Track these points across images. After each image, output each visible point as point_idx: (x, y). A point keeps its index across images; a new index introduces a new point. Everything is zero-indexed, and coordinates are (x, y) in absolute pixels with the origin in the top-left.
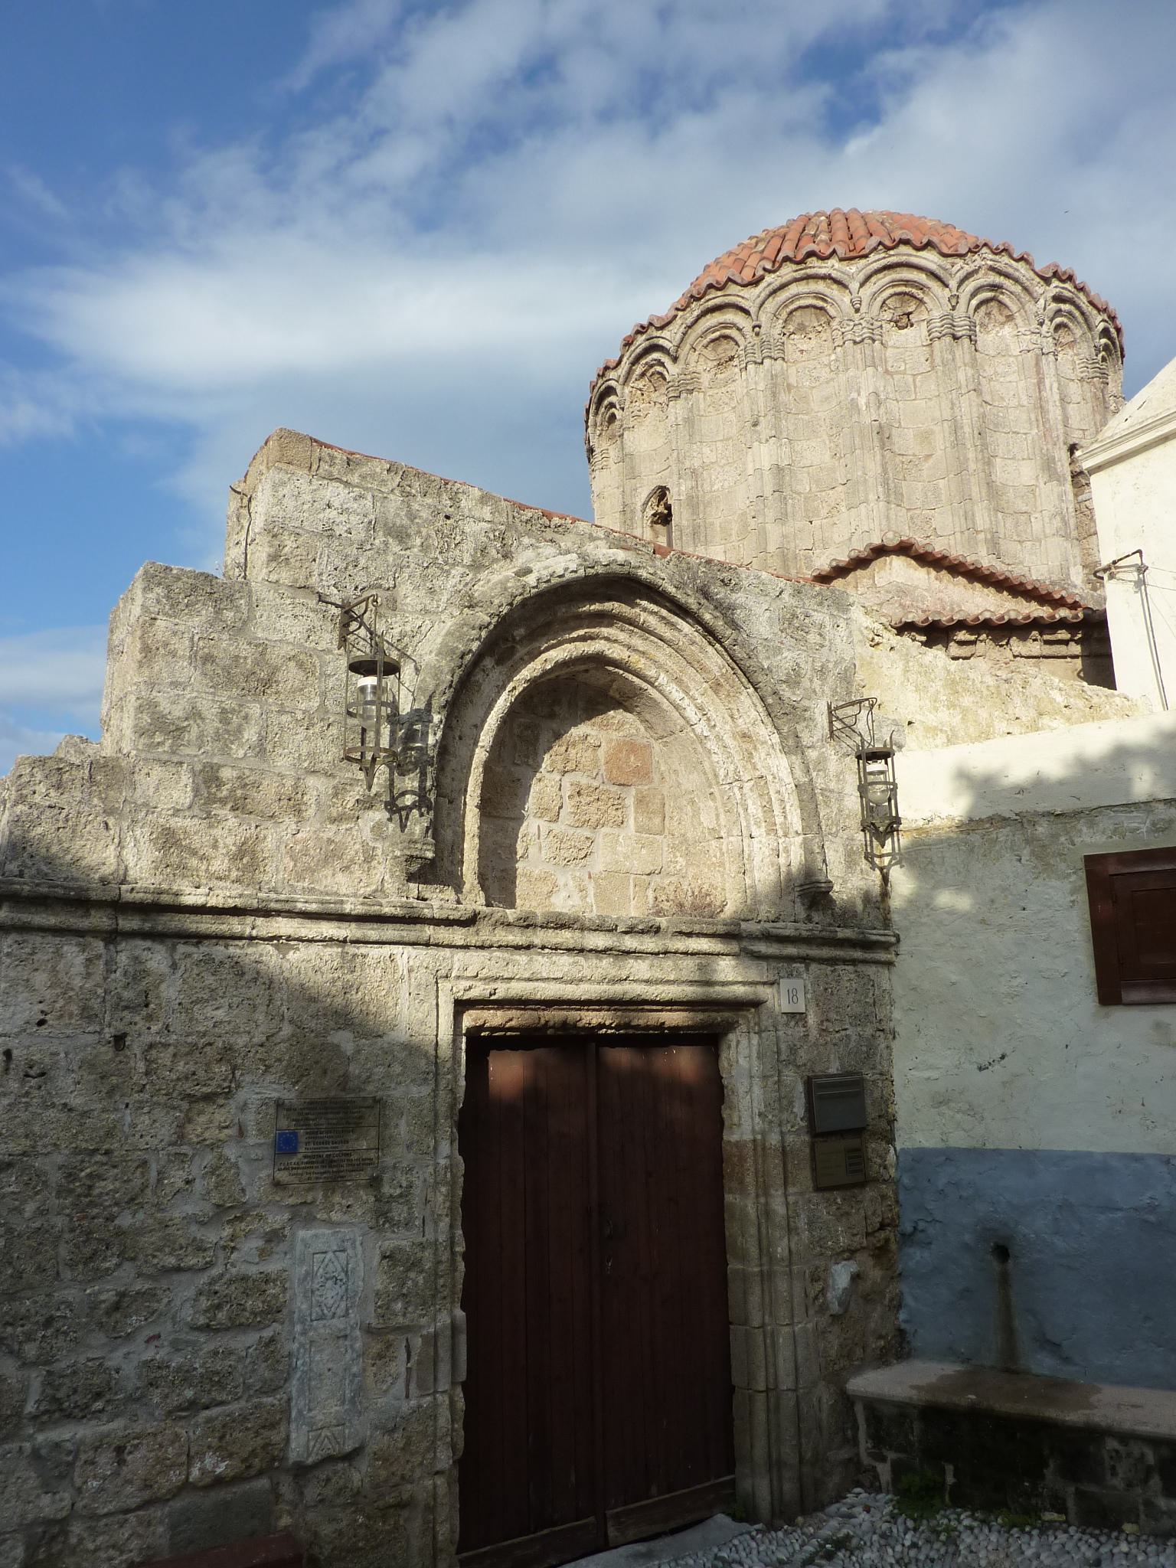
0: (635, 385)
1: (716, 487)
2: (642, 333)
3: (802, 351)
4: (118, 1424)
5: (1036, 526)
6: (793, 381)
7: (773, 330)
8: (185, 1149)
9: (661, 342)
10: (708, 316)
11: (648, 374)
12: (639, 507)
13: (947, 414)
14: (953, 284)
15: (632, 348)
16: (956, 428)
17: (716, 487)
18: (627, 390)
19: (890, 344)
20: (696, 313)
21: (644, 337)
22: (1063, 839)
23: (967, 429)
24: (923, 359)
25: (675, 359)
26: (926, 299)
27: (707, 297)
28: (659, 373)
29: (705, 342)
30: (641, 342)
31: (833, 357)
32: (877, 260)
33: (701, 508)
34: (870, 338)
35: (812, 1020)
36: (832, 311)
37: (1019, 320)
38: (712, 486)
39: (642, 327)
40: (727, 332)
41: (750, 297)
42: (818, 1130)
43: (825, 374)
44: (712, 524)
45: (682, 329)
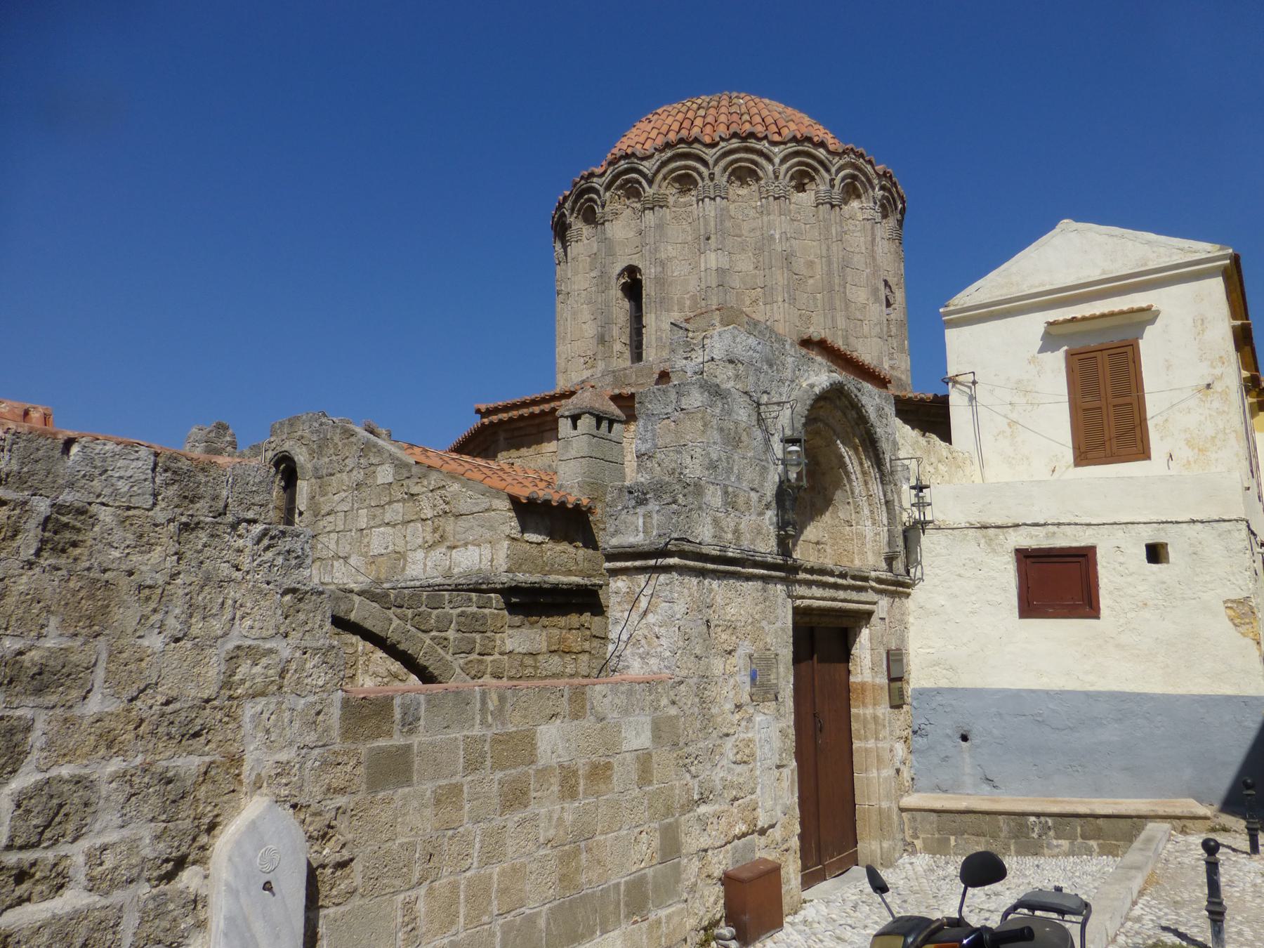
1: (675, 274)
4: (717, 807)
5: (866, 328)
6: (732, 213)
7: (722, 180)
8: (726, 677)
9: (641, 167)
13: (824, 253)
14: (833, 170)
15: (616, 166)
16: (829, 263)
17: (675, 274)
18: (608, 194)
19: (793, 201)
22: (1001, 537)
23: (835, 265)
24: (811, 215)
25: (650, 183)
26: (816, 177)
30: (623, 165)
31: (759, 203)
32: (792, 147)
34: (784, 196)
35: (887, 620)
36: (761, 173)
37: (863, 199)
38: (673, 272)
41: (710, 155)
42: (893, 676)
43: (752, 213)
44: (672, 298)
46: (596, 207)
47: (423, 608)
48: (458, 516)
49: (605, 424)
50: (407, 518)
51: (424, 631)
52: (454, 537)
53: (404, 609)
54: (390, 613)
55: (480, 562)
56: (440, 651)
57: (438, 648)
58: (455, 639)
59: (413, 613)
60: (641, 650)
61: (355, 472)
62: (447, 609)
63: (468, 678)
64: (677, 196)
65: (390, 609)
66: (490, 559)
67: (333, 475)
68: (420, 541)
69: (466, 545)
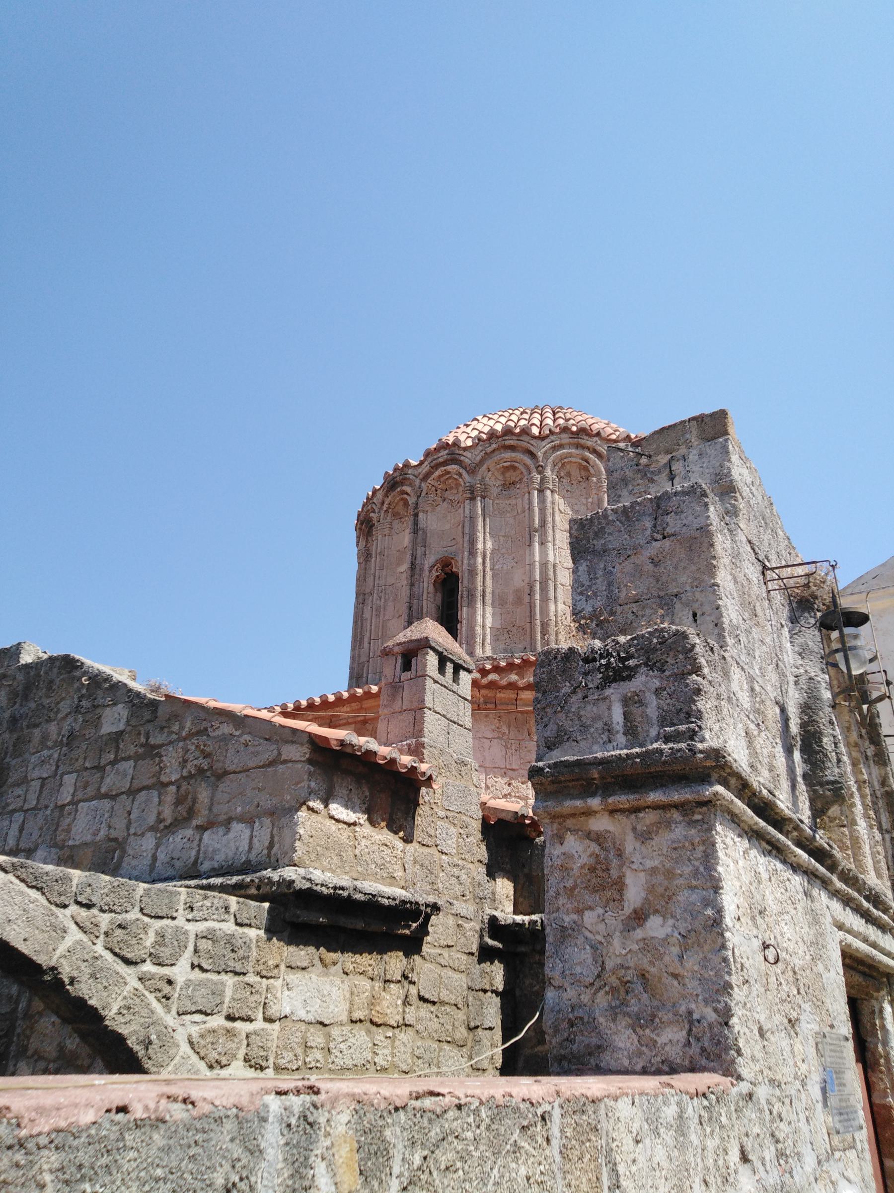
2: (445, 449)
3: (567, 491)
12: (426, 567)
21: (447, 451)
46: (408, 498)
47: (134, 914)
48: (222, 775)
49: (449, 668)
50: (137, 784)
51: (128, 962)
52: (210, 809)
53: (95, 911)
54: (64, 916)
55: (250, 848)
56: (155, 1005)
57: (151, 998)
58: (188, 984)
59: (111, 922)
60: (634, 1008)
61: (70, 720)
62: (180, 922)
63: (202, 1065)
65: (65, 906)
66: (267, 844)
67: (36, 726)
68: (152, 819)
69: (229, 821)
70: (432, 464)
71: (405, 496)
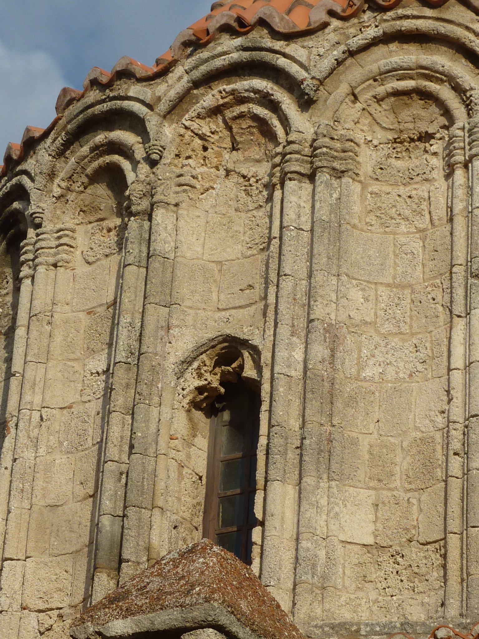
0: (194, 126)
1: (367, 373)
9: (282, 62)
10: (393, 46)
11: (229, 114)
15: (205, 54)
17: (367, 373)
20: (371, 33)
21: (238, 41)
27: (400, 11)
28: (256, 118)
29: (381, 90)
33: (339, 405)
38: (361, 367)
39: (240, 21)
40: (432, 86)
44: (354, 442)
45: (337, 53)
46: (126, 165)
64: (386, 150)
70: (197, 74)
71: (116, 158)
